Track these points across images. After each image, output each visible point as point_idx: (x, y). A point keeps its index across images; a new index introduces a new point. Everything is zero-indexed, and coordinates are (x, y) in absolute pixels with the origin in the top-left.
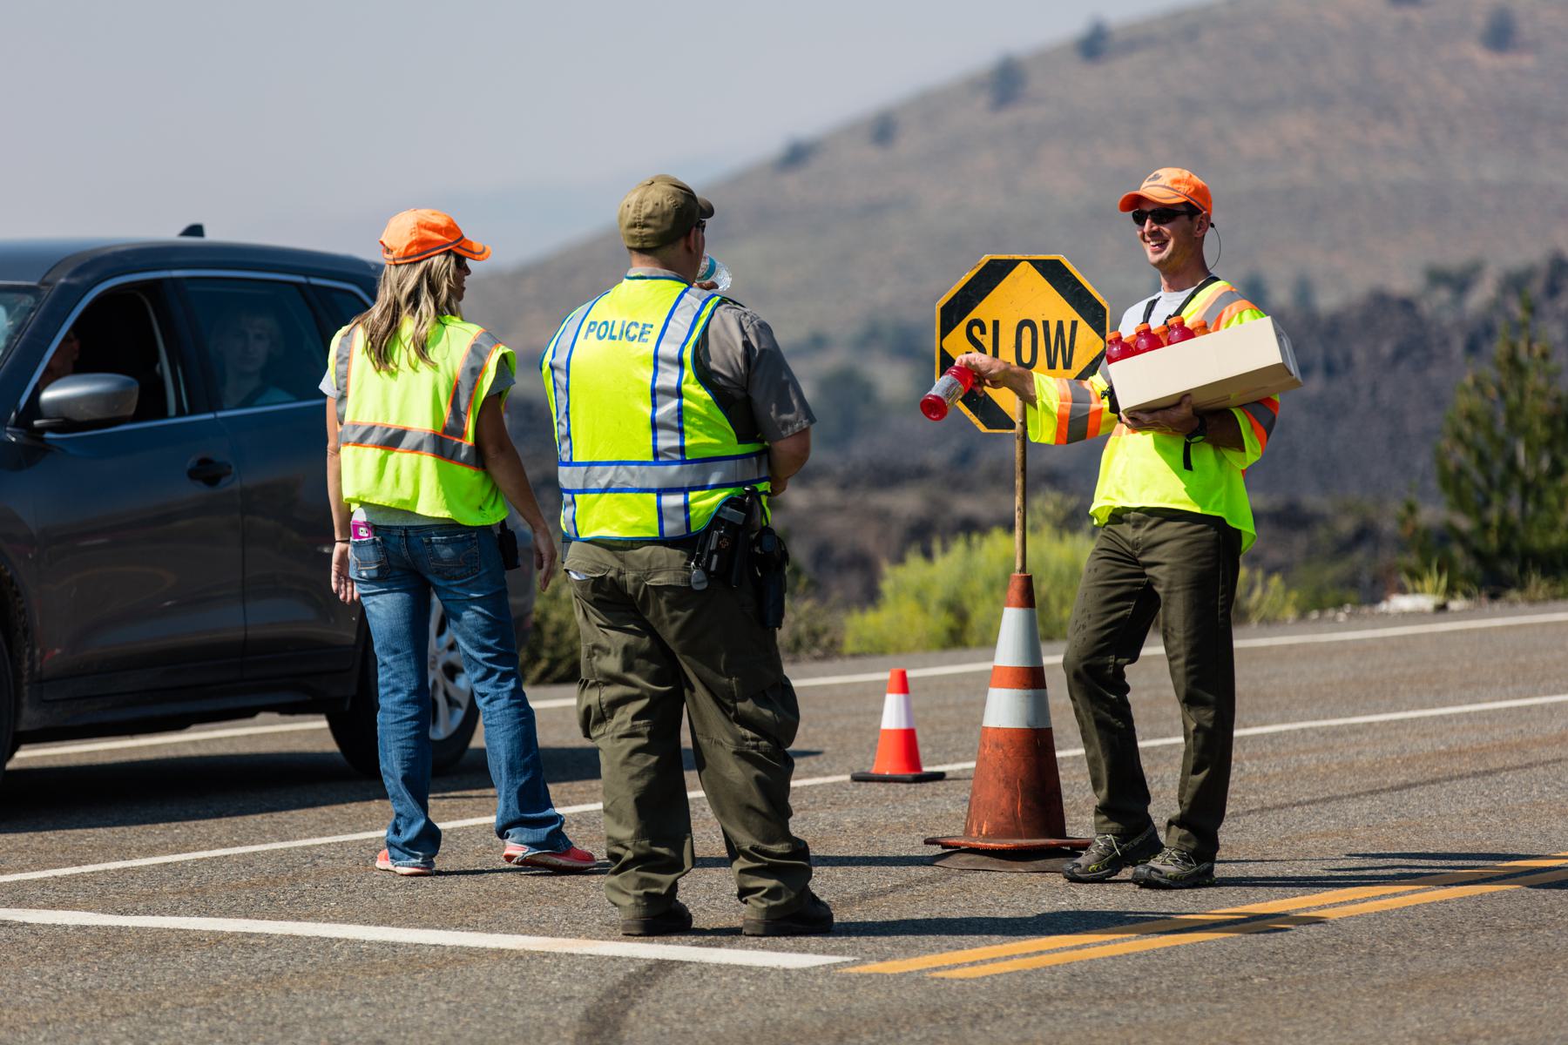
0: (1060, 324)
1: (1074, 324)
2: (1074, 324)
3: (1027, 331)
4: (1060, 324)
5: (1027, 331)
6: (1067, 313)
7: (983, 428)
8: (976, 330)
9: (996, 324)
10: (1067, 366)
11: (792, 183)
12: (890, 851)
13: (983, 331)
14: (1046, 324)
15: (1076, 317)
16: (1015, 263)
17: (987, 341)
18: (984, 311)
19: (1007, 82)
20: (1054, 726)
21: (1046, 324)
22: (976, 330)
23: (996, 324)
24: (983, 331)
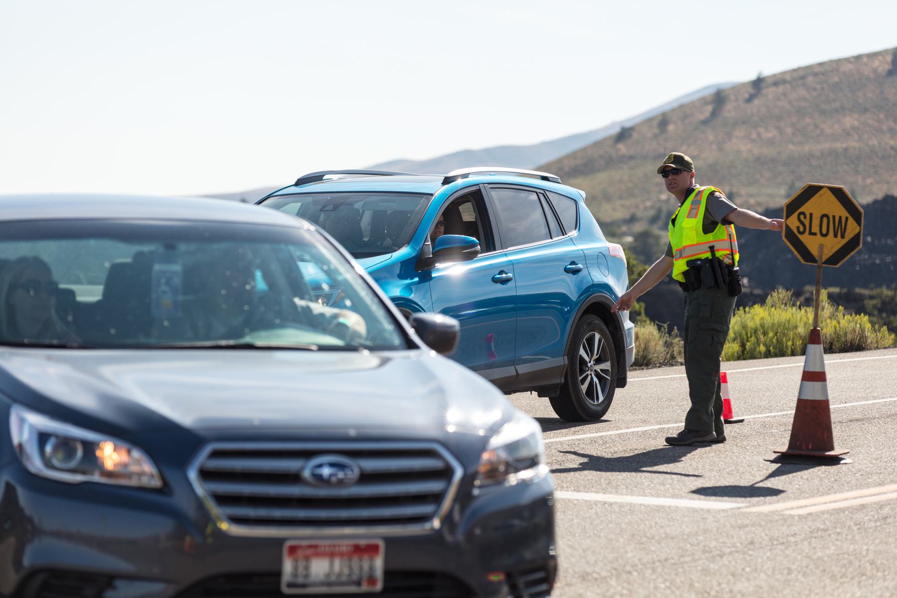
0: (840, 218)
1: (847, 218)
2: (847, 218)
3: (825, 219)
4: (840, 218)
5: (825, 219)
6: (844, 213)
7: (802, 261)
8: (802, 217)
9: (811, 215)
10: (843, 237)
11: (622, 148)
12: (668, 476)
13: (805, 218)
14: (834, 217)
15: (848, 215)
16: (821, 188)
17: (807, 222)
18: (806, 208)
19: (719, 98)
20: (830, 398)
21: (834, 217)
22: (802, 217)
23: (811, 215)
24: (805, 218)
